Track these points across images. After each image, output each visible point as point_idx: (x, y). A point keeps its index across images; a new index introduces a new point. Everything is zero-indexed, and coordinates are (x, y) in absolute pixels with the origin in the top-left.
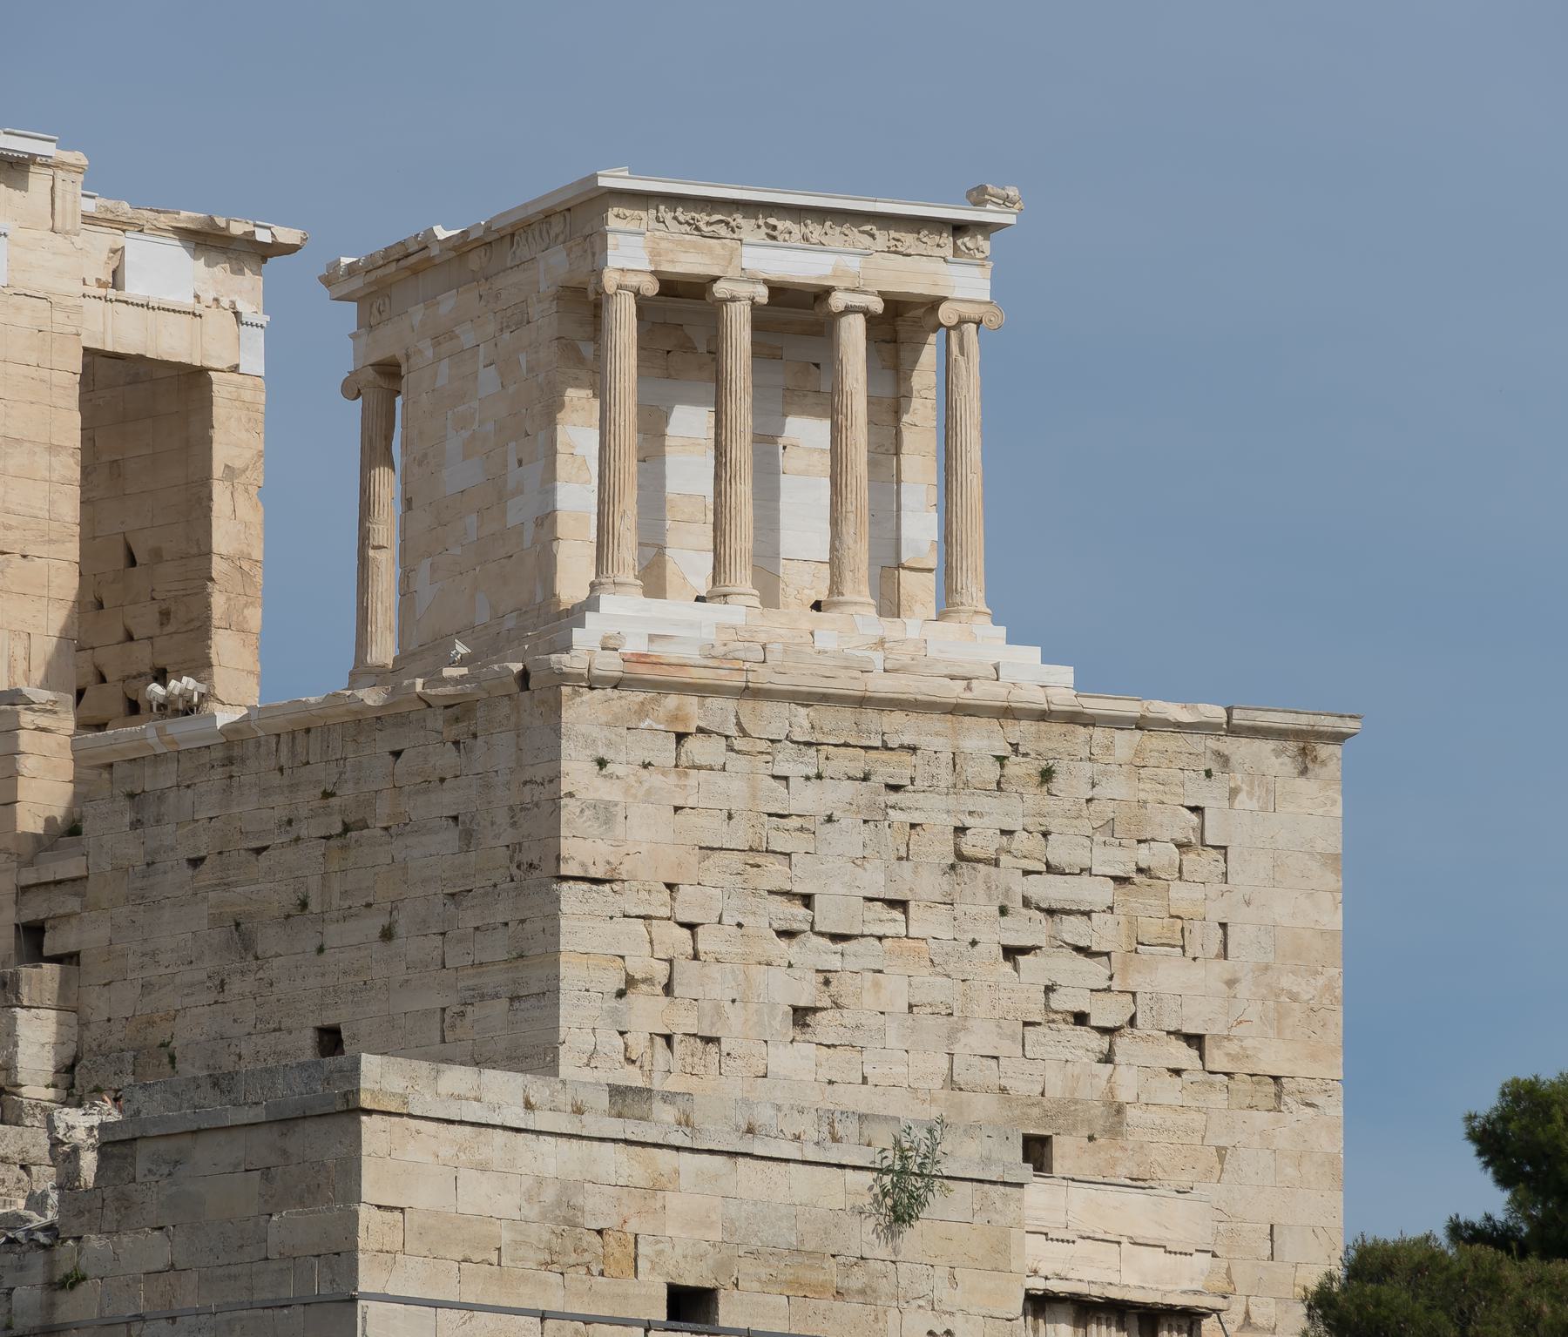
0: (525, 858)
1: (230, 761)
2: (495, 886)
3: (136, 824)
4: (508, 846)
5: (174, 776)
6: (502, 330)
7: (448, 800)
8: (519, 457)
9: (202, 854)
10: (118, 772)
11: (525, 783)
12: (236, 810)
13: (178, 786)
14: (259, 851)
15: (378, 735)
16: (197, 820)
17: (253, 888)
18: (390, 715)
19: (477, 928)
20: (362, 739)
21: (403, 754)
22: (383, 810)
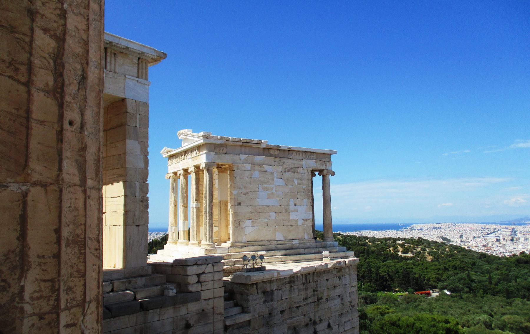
0: (352, 304)
1: (290, 282)
2: (348, 311)
3: (265, 302)
4: (349, 302)
5: (276, 287)
6: (285, 171)
7: (338, 291)
8: (295, 203)
9: (284, 309)
10: (259, 286)
11: (352, 287)
12: (293, 296)
13: (277, 289)
14: (297, 307)
15: (324, 275)
16: (282, 300)
17: (298, 318)
18: (326, 270)
19: (345, 322)
20: (321, 276)
21: (329, 280)
22: (325, 294)
